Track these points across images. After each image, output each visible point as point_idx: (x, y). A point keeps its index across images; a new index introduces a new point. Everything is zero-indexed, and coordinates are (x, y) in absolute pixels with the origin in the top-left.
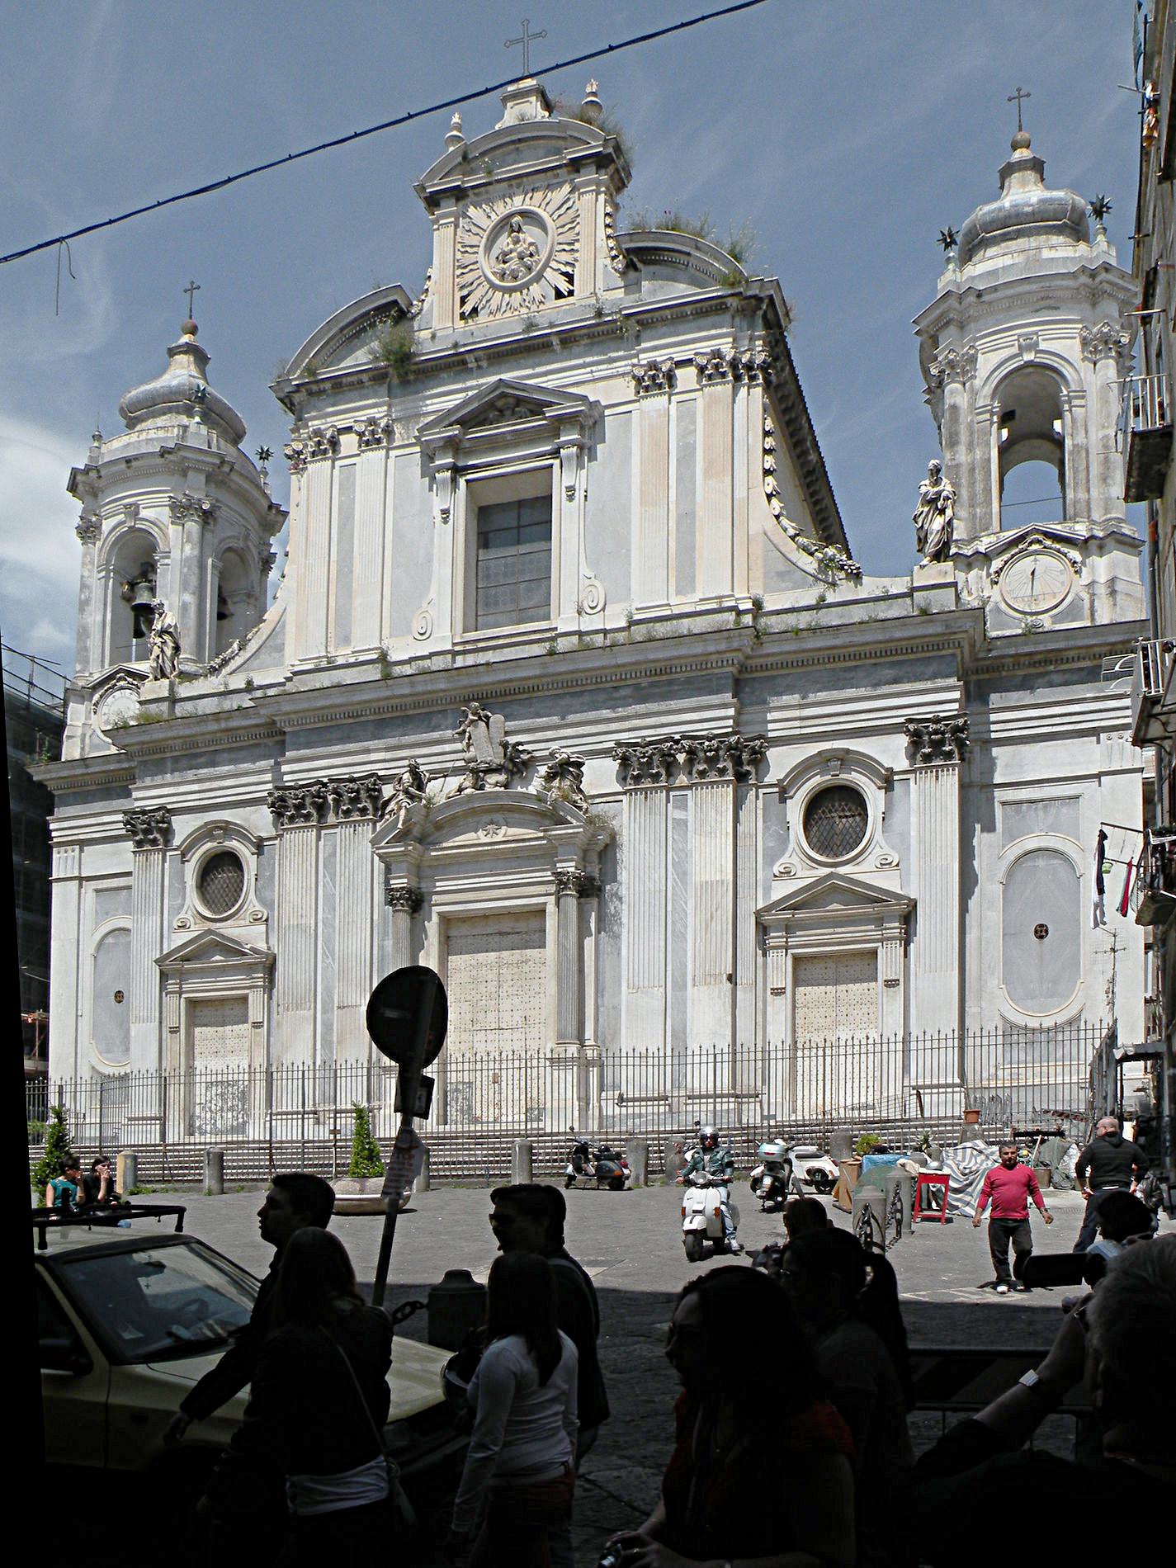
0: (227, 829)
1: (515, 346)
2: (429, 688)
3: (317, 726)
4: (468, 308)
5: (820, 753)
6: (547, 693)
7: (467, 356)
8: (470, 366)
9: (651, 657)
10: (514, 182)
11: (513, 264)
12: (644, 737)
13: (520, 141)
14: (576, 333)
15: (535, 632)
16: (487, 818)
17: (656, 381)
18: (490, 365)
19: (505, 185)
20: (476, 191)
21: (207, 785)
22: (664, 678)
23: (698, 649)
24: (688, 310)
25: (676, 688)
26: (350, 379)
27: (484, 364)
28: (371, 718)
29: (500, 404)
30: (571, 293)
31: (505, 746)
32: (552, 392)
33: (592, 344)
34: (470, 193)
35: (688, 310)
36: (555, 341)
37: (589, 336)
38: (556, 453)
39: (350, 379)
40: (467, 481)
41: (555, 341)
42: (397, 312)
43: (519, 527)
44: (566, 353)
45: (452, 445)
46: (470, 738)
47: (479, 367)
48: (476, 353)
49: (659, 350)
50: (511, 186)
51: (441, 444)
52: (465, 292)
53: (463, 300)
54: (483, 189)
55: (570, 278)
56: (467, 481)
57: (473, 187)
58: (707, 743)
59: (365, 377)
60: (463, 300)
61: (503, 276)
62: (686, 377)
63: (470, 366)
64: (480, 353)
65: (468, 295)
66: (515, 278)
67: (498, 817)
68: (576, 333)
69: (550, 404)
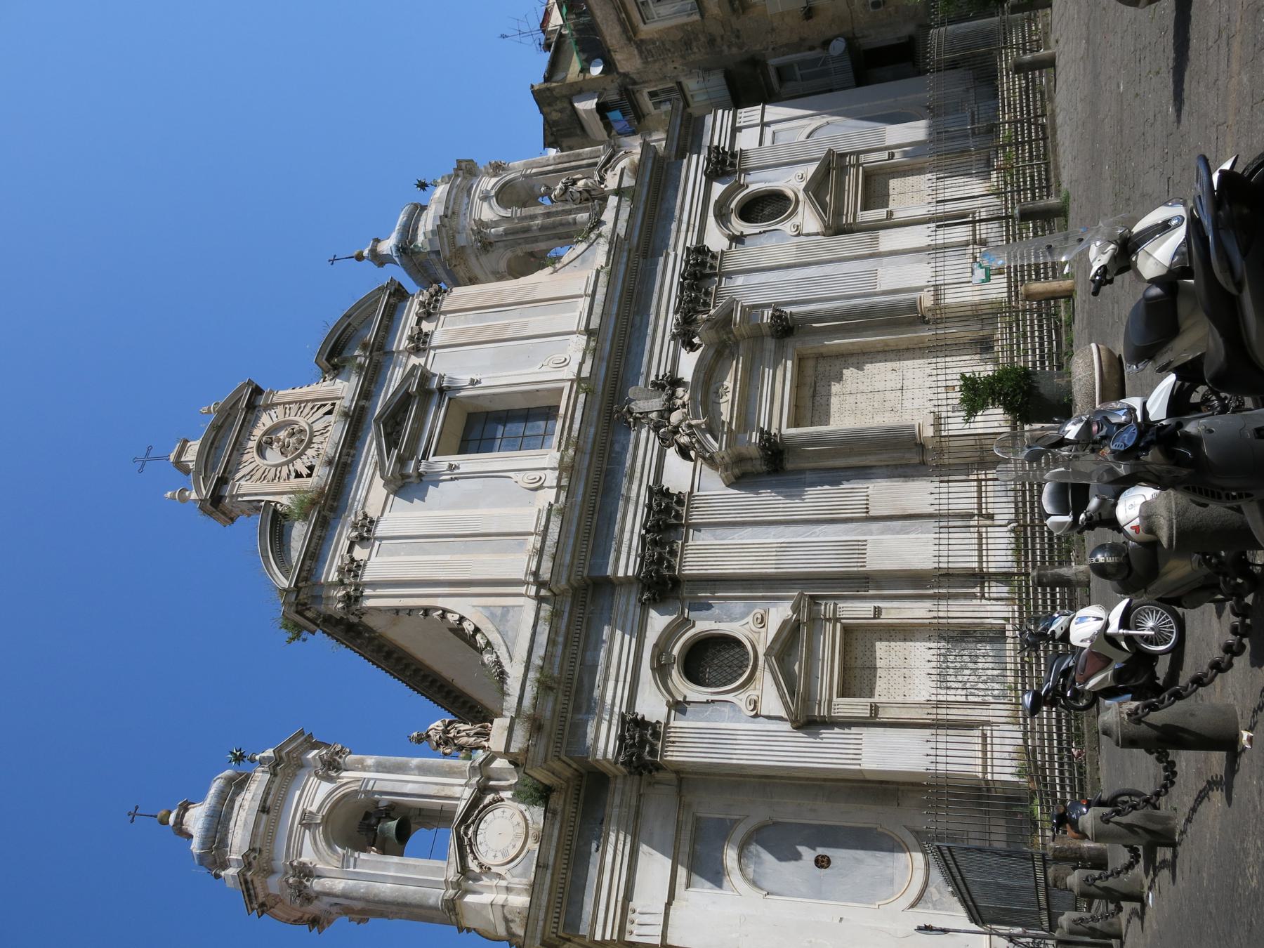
0: (661, 648)
1: (352, 427)
2: (590, 440)
3: (590, 547)
4: (305, 471)
5: (715, 216)
6: (622, 369)
7: (342, 460)
8: (349, 462)
9: (618, 294)
10: (237, 446)
11: (293, 440)
12: (676, 296)
13: (212, 443)
14: (365, 387)
15: (569, 397)
16: (712, 397)
17: (420, 343)
18: (355, 449)
19: (235, 452)
20: (228, 470)
21: (613, 671)
22: (635, 296)
23: (622, 268)
24: (381, 333)
25: (644, 290)
26: (313, 545)
27: (352, 452)
28: (599, 499)
29: (389, 430)
30: (333, 404)
31: (654, 384)
32: (401, 385)
33: (376, 383)
34: (226, 475)
35: (385, 322)
36: (362, 403)
37: (370, 383)
38: (442, 391)
39: (313, 545)
40: (434, 455)
41: (362, 403)
42: (278, 523)
43: (481, 440)
44: (374, 398)
45: (402, 461)
46: (641, 413)
47: (354, 456)
48: (343, 454)
49: (402, 341)
50: (238, 450)
51: (399, 465)
52: (293, 474)
53: (298, 475)
54: (229, 467)
55: (325, 405)
56: (434, 455)
57: (224, 471)
58: (691, 262)
59: (318, 533)
60: (298, 475)
61: (297, 449)
62: (426, 326)
63: (349, 462)
64: (345, 451)
65: (296, 472)
66: (303, 441)
67: (713, 388)
68: (365, 387)
69: (407, 391)
